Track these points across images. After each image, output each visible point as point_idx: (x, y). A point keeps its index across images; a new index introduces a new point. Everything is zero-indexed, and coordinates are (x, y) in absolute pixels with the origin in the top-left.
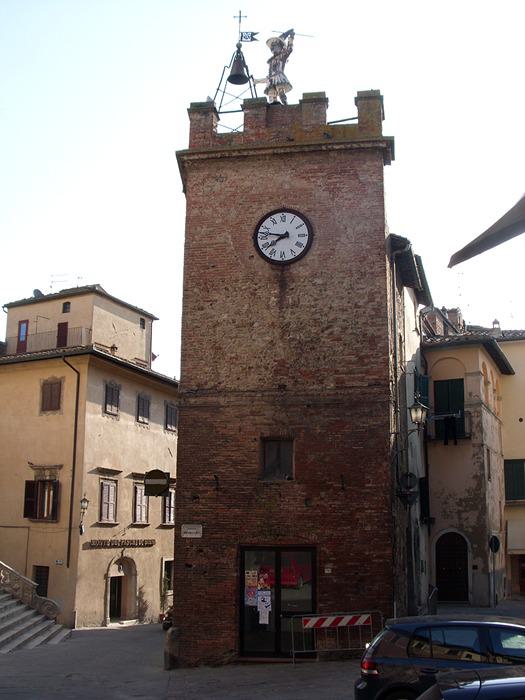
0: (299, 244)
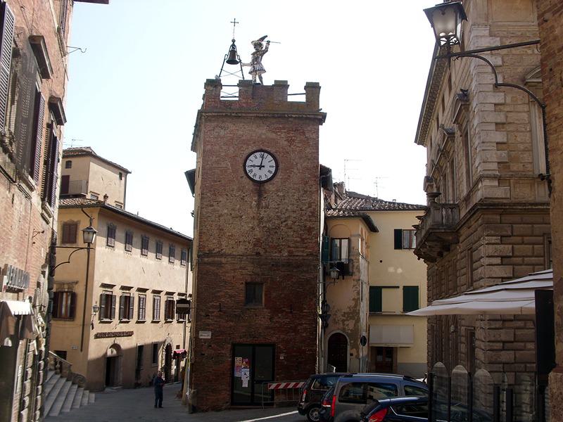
0: (269, 171)
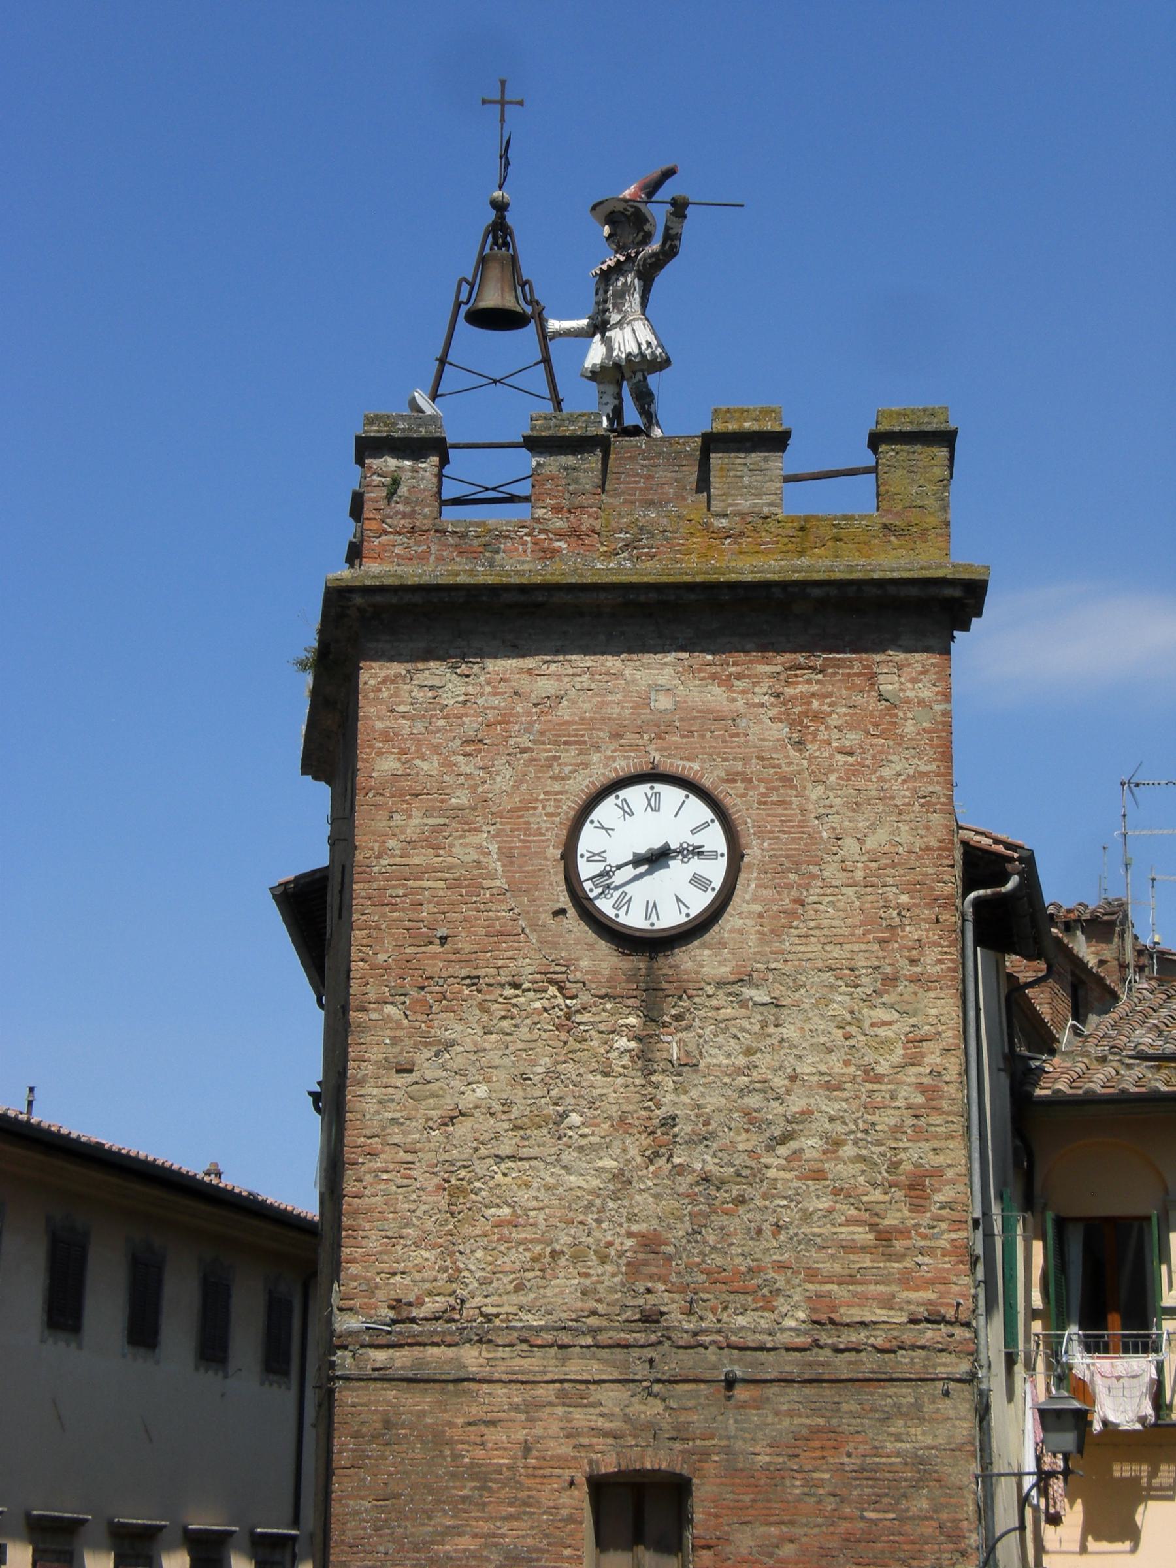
0: (698, 881)
